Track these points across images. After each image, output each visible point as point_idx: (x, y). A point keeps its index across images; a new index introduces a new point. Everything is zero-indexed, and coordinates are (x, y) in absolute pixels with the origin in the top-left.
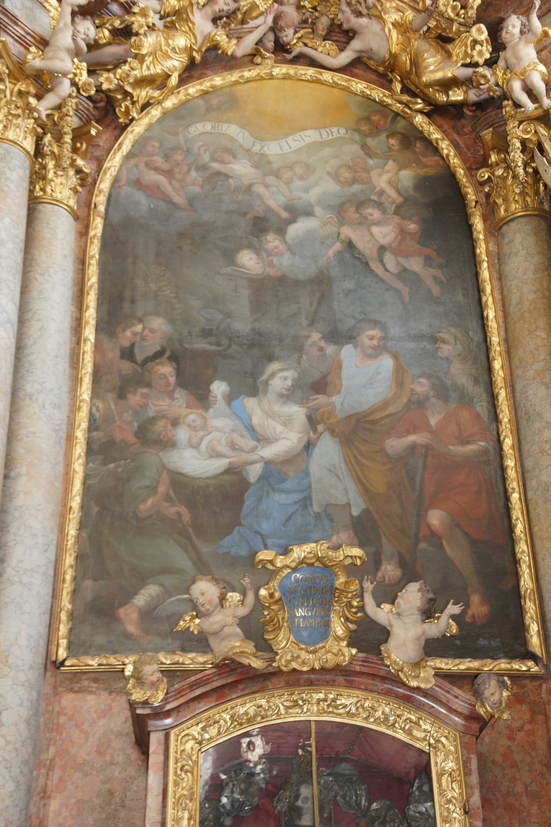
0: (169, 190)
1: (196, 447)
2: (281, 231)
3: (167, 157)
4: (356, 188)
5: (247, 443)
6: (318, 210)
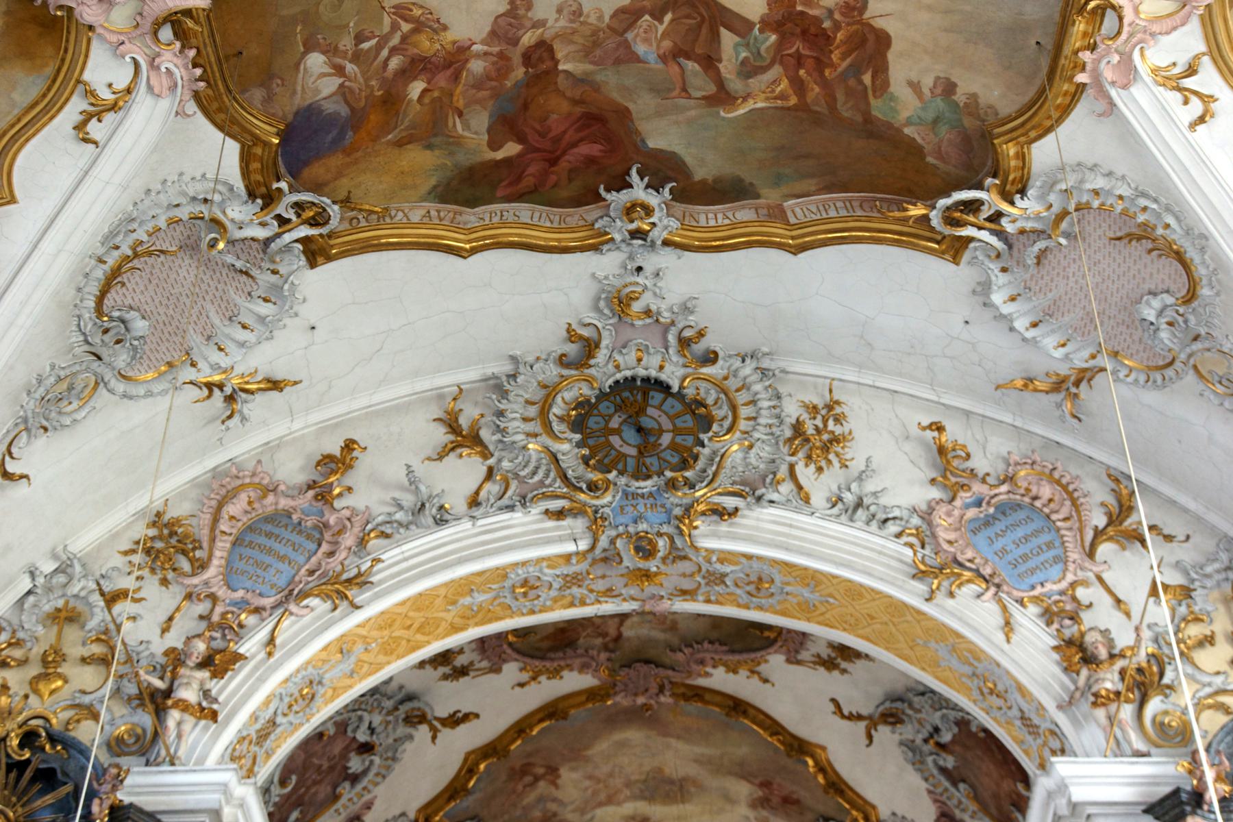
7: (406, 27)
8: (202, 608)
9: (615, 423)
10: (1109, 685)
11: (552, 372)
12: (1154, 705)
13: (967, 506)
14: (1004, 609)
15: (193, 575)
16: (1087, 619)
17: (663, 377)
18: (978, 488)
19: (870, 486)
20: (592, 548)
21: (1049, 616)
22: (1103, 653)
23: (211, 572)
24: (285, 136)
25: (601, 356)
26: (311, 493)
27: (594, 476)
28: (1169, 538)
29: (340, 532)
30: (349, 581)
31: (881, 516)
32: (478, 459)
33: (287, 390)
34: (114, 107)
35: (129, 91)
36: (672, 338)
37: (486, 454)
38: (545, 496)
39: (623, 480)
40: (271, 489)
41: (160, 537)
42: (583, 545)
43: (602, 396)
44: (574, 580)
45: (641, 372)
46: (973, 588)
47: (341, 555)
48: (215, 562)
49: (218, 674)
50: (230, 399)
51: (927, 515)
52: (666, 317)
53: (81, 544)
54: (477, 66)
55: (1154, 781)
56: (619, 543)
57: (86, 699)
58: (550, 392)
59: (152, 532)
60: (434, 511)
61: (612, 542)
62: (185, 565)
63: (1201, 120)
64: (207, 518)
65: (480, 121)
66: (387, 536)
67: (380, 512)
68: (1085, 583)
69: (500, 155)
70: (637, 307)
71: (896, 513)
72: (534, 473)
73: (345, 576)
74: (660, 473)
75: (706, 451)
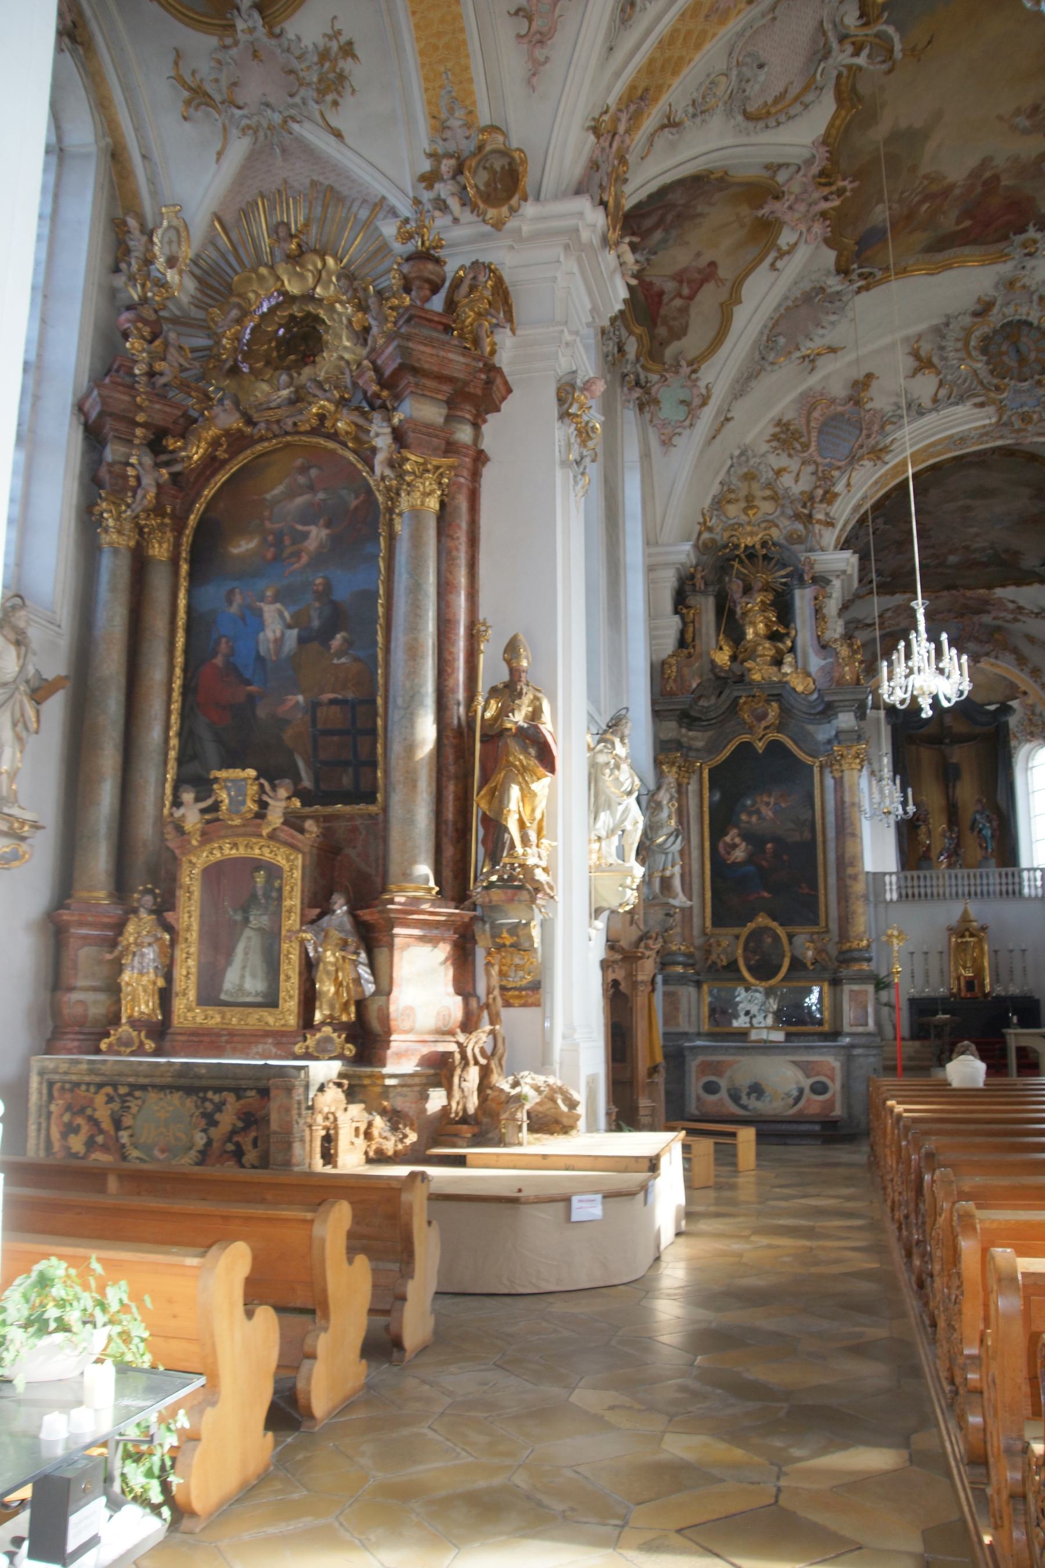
7: (926, 182)
8: (811, 468)
9: (1004, 348)
11: (968, 320)
17: (1030, 319)
20: (998, 423)
23: (812, 449)
24: (857, 243)
25: (995, 310)
27: (996, 381)
29: (871, 423)
30: (881, 450)
33: (839, 353)
34: (788, 252)
35: (796, 244)
36: (1035, 297)
37: (938, 373)
39: (1013, 383)
40: (833, 401)
41: (782, 432)
42: (994, 420)
43: (995, 332)
44: (986, 434)
45: (1017, 317)
48: (813, 444)
49: (830, 503)
50: (813, 361)
52: (1033, 288)
53: (748, 439)
54: (957, 192)
56: (1013, 419)
57: (770, 518)
58: (968, 332)
59: (778, 429)
62: (798, 447)
64: (803, 421)
65: (953, 215)
66: (894, 423)
67: (888, 409)
69: (961, 227)
70: (1018, 284)
72: (965, 381)
74: (1032, 377)
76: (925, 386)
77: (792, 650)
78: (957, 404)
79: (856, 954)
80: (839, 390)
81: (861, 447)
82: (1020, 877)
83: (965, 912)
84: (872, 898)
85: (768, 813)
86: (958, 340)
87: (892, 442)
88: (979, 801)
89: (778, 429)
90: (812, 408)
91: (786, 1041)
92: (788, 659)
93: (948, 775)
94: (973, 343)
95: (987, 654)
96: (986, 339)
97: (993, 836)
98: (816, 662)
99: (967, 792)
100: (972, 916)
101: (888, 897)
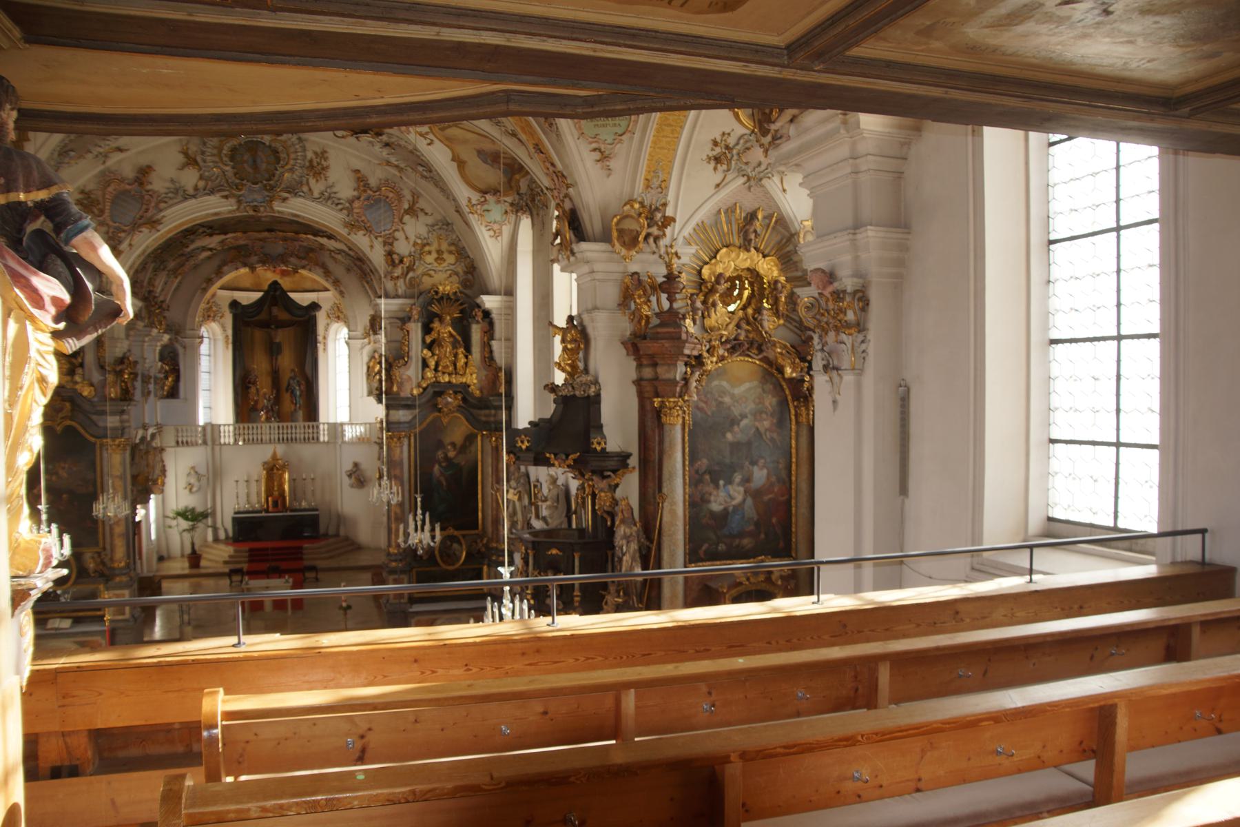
0: (706, 409)
1: (716, 502)
2: (738, 424)
3: (705, 396)
4: (760, 406)
5: (729, 500)
6: (749, 416)
10: (396, 275)
12: (411, 274)
13: (364, 200)
14: (371, 241)
15: (99, 216)
16: (396, 244)
18: (369, 192)
19: (334, 190)
20: (238, 209)
21: (385, 243)
22: (397, 262)
23: (107, 213)
26: (136, 184)
28: (426, 214)
30: (154, 222)
31: (337, 201)
32: (196, 171)
37: (200, 169)
38: (220, 191)
39: (249, 184)
40: (122, 180)
42: (235, 208)
43: (240, 145)
46: (362, 232)
47: (151, 209)
51: (351, 202)
55: (404, 304)
60: (182, 193)
61: (245, 208)
62: (96, 211)
63: (429, 144)
64: (100, 193)
66: (166, 202)
68: (397, 230)
71: (342, 201)
72: (217, 179)
73: (155, 219)
74: (261, 182)
75: (278, 172)
76: (190, 178)
77: (82, 365)
78: (209, 195)
79: (117, 572)
80: (129, 172)
81: (141, 217)
82: (318, 427)
83: (274, 455)
84: (209, 442)
85: (64, 474)
86: (215, 147)
87: (164, 217)
88: (293, 370)
89: (80, 196)
90: (108, 184)
91: (71, 627)
92: (79, 371)
93: (273, 350)
94: (224, 152)
95: (303, 267)
96: (234, 150)
97: (300, 395)
98: (96, 377)
99: (286, 361)
100: (278, 457)
101: (222, 441)
